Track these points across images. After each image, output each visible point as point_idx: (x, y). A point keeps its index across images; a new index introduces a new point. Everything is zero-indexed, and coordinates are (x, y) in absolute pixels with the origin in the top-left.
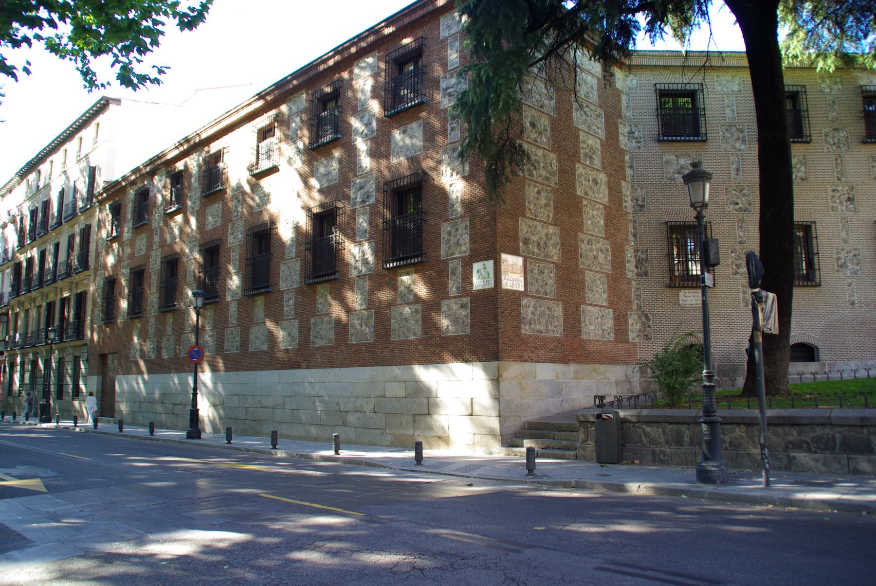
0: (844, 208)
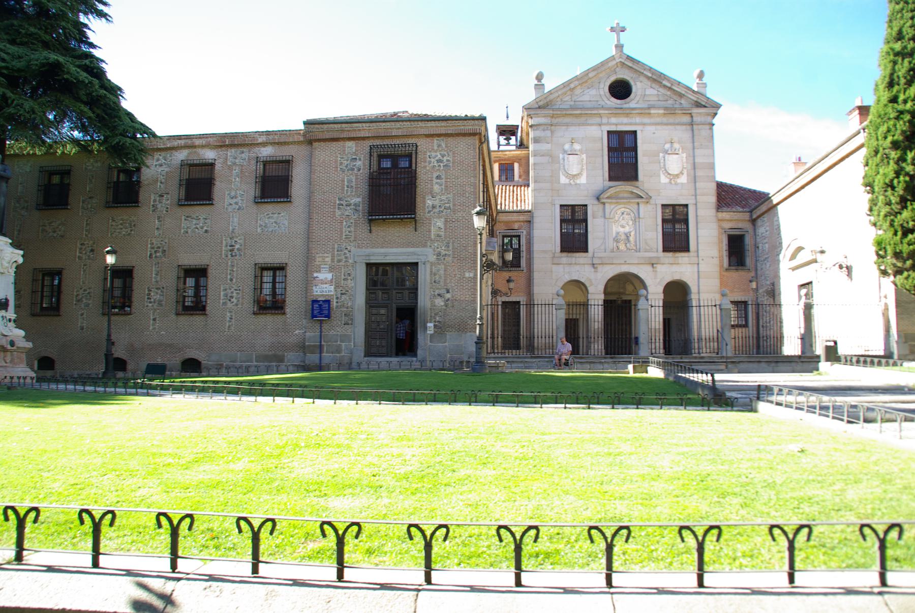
0: (87, 257)
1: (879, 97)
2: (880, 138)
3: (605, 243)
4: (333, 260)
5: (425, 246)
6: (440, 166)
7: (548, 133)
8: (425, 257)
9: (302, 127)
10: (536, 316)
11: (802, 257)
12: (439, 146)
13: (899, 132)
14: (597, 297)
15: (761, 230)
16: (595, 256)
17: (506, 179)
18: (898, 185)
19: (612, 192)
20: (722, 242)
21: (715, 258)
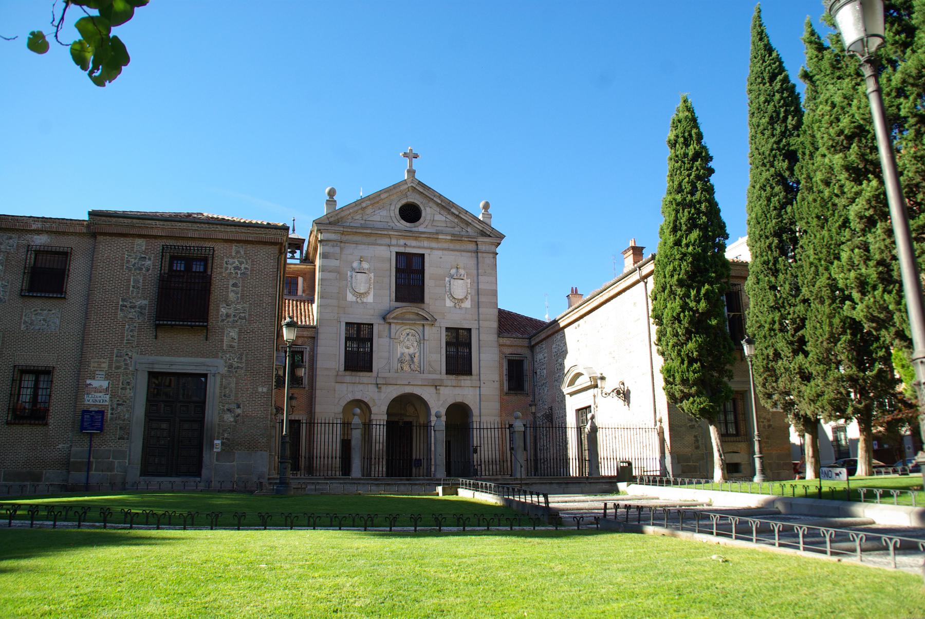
1: (665, 240)
2: (667, 276)
3: (390, 363)
4: (110, 367)
5: (216, 357)
6: (237, 273)
7: (337, 250)
8: (216, 368)
9: (86, 218)
10: (316, 436)
11: (583, 382)
12: (238, 252)
13: (683, 271)
14: (380, 414)
15: (539, 357)
16: (379, 376)
17: (290, 293)
18: (684, 319)
19: (398, 313)
20: (503, 366)
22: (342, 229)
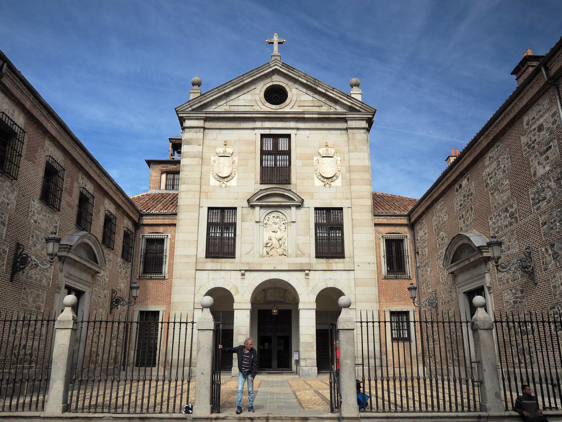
7: (200, 135)
17: (173, 188)
21: (371, 264)
22: (204, 115)
